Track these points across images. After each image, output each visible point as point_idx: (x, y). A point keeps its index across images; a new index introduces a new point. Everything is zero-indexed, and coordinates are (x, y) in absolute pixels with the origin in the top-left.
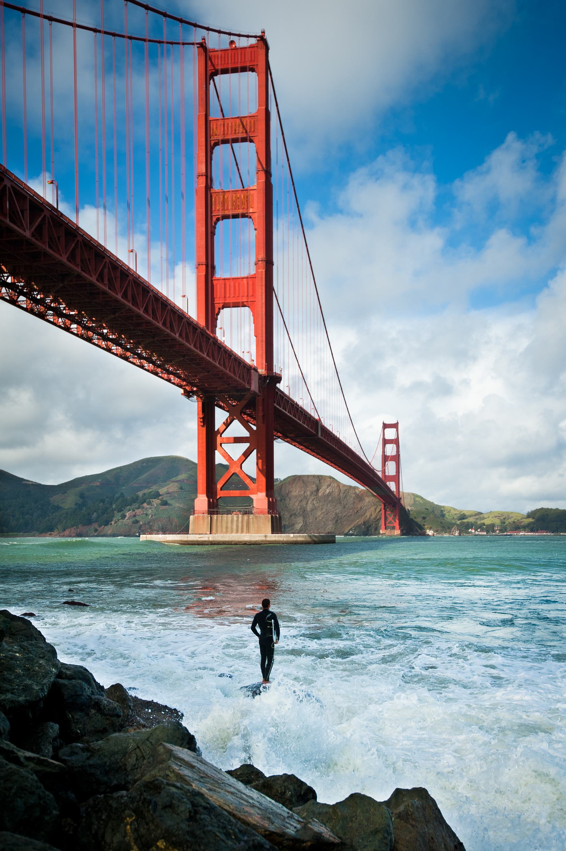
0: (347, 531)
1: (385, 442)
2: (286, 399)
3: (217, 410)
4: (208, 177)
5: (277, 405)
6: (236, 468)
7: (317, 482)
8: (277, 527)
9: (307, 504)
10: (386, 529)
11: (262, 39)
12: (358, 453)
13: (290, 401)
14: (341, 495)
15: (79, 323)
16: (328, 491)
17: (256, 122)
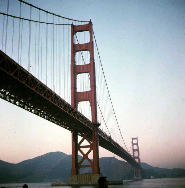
1: (133, 144)
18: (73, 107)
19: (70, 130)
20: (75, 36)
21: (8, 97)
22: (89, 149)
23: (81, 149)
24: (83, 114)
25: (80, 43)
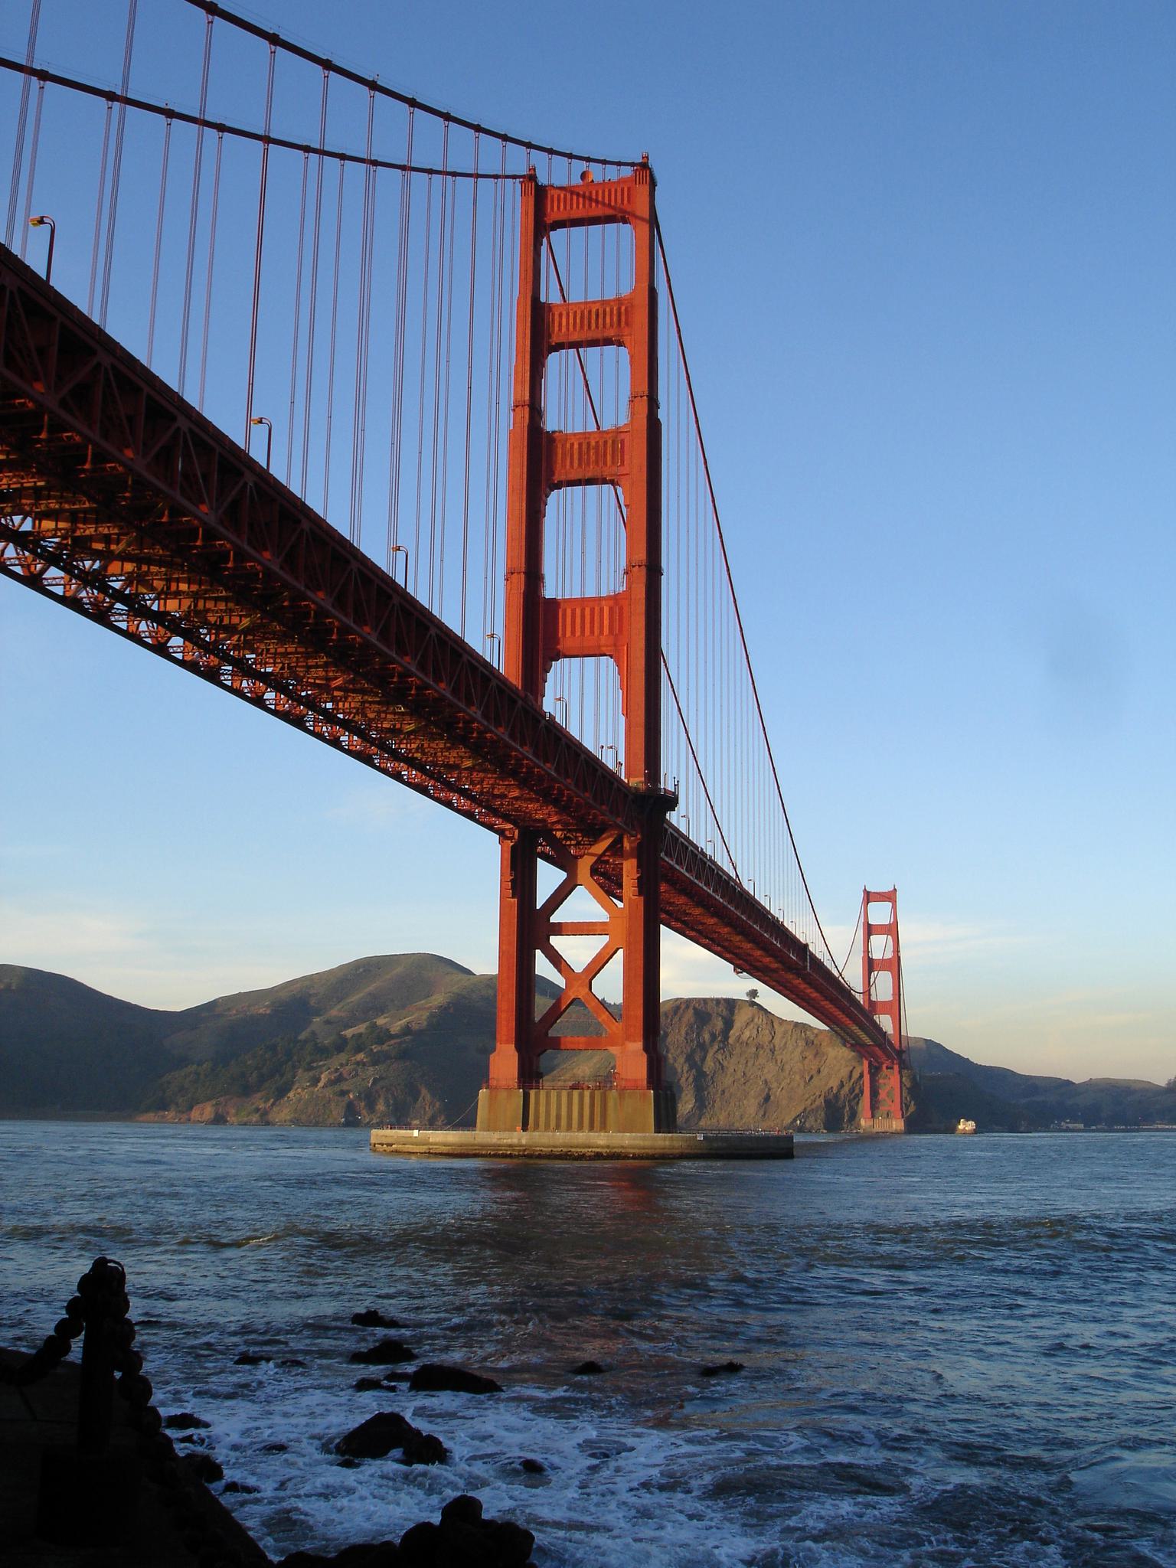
0: (789, 1121)
2: (682, 843)
3: (541, 864)
4: (534, 408)
5: (666, 855)
6: (580, 988)
7: (725, 1013)
8: (665, 1120)
9: (703, 1059)
10: (873, 1116)
11: (644, 166)
12: (819, 956)
13: (690, 848)
14: (776, 1041)
15: (187, 635)
16: (747, 1033)
17: (629, 309)
18: (515, 679)
19: (490, 827)
20: (545, 240)
21: (118, 605)
22: (598, 943)
23: (555, 941)
24: (574, 731)
25: (575, 296)
